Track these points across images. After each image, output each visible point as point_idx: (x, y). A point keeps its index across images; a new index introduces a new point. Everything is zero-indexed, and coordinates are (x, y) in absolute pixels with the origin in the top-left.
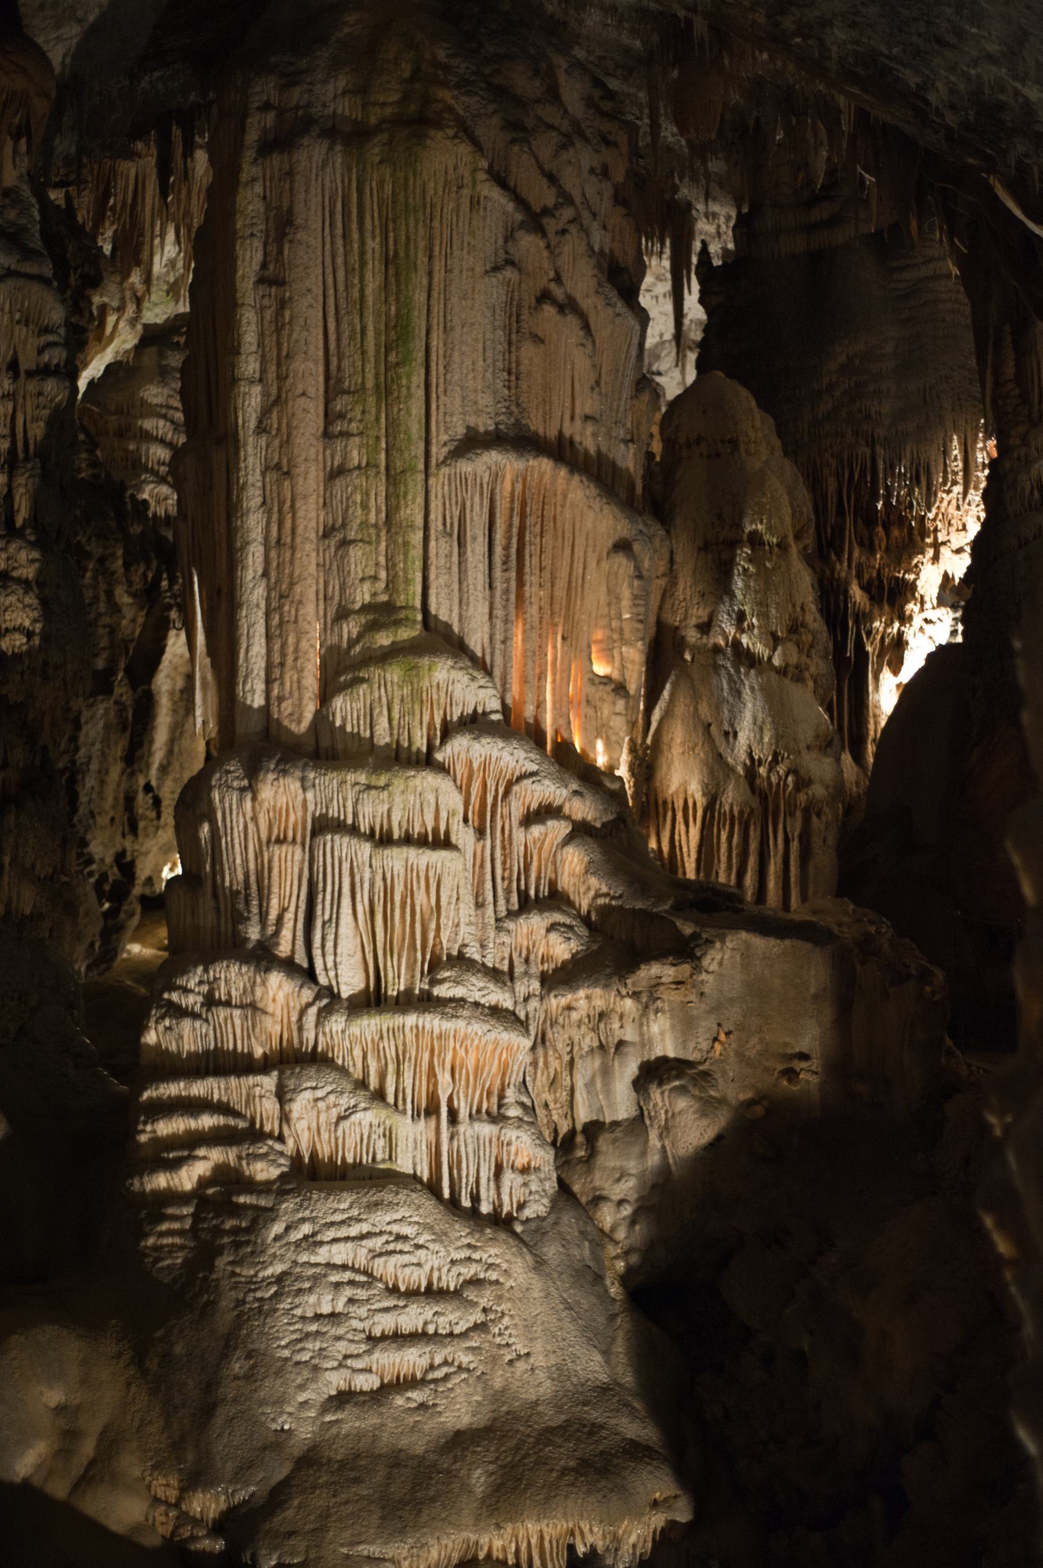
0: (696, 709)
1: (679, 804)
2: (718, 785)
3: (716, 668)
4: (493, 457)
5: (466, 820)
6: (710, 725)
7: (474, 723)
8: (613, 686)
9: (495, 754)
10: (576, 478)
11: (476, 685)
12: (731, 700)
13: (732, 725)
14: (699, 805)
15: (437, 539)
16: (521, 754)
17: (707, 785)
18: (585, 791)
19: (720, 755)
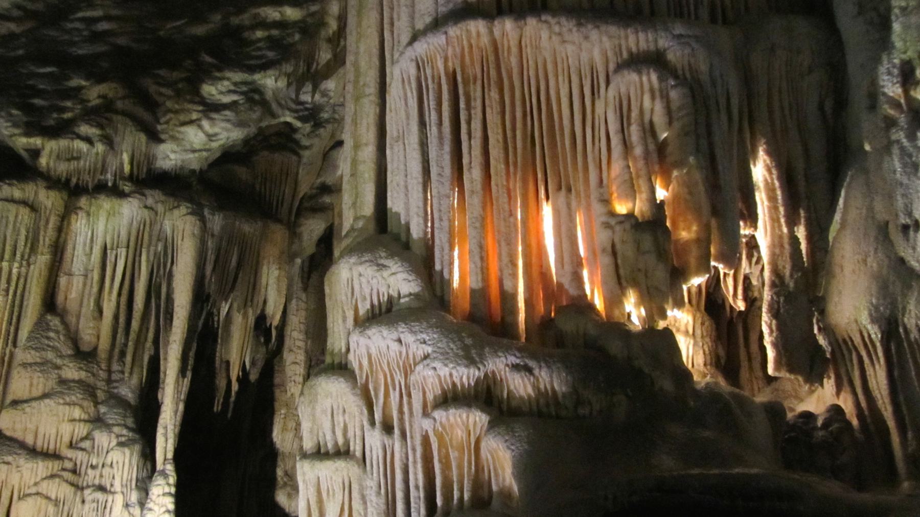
0: (871, 209)
1: (857, 340)
2: (893, 304)
3: (887, 149)
4: (420, 47)
5: (372, 423)
6: (887, 223)
7: (384, 313)
8: (633, 221)
9: (383, 345)
10: (531, 22)
11: (386, 273)
12: (905, 181)
13: (910, 214)
14: (873, 336)
15: (392, 148)
16: (408, 338)
17: (876, 308)
18: (532, 363)
19: (902, 261)
